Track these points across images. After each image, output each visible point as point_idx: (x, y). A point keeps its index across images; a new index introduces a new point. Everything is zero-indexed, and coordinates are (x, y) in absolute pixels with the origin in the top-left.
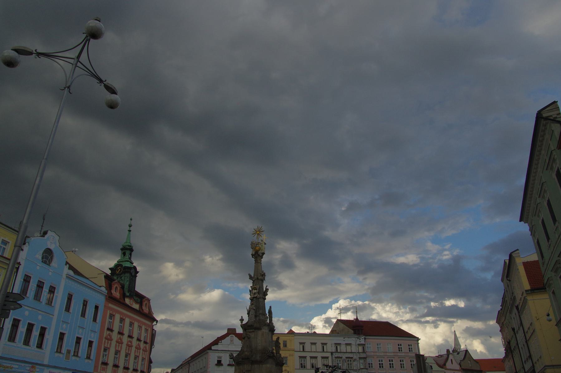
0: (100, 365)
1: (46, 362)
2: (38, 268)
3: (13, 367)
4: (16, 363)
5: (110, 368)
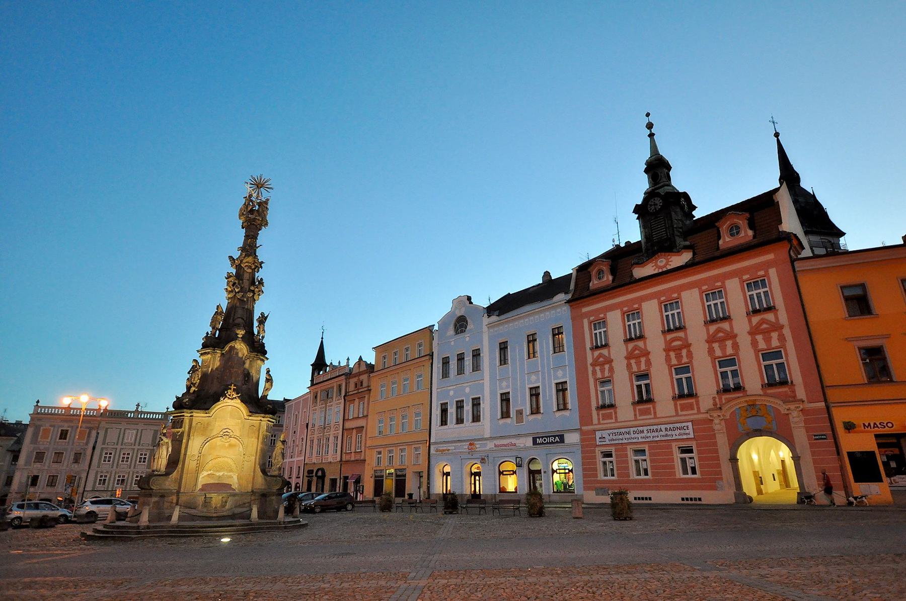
0: (594, 413)
1: (487, 435)
2: (452, 343)
3: (449, 450)
4: (450, 445)
5: (625, 410)
